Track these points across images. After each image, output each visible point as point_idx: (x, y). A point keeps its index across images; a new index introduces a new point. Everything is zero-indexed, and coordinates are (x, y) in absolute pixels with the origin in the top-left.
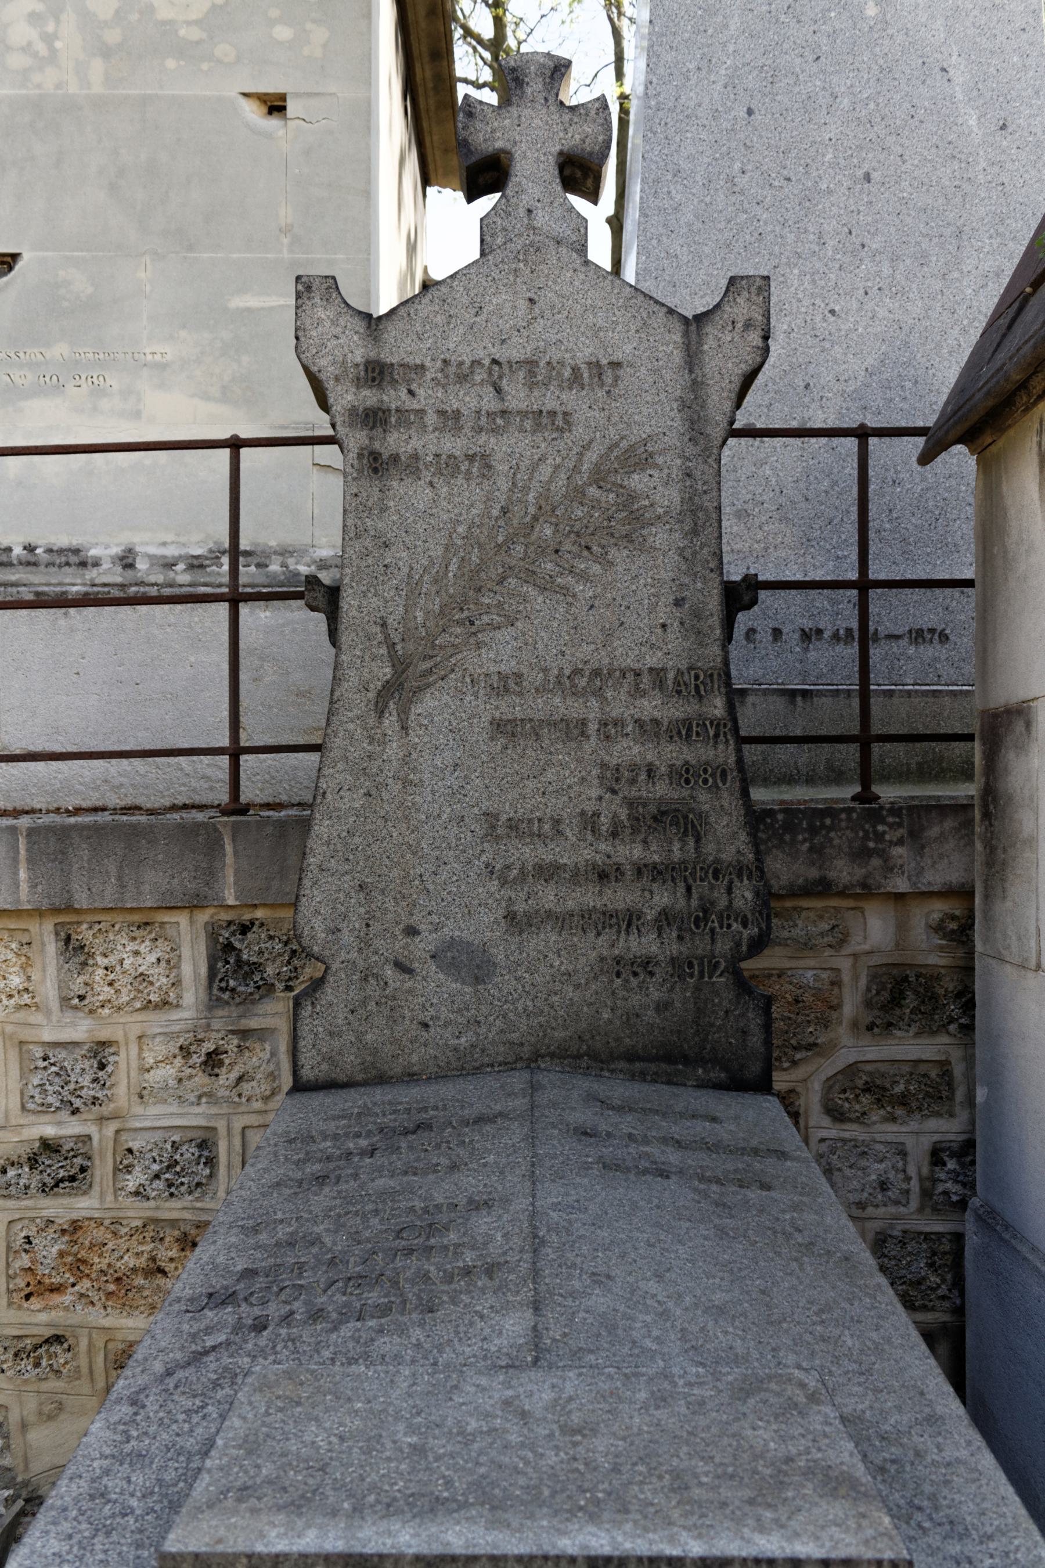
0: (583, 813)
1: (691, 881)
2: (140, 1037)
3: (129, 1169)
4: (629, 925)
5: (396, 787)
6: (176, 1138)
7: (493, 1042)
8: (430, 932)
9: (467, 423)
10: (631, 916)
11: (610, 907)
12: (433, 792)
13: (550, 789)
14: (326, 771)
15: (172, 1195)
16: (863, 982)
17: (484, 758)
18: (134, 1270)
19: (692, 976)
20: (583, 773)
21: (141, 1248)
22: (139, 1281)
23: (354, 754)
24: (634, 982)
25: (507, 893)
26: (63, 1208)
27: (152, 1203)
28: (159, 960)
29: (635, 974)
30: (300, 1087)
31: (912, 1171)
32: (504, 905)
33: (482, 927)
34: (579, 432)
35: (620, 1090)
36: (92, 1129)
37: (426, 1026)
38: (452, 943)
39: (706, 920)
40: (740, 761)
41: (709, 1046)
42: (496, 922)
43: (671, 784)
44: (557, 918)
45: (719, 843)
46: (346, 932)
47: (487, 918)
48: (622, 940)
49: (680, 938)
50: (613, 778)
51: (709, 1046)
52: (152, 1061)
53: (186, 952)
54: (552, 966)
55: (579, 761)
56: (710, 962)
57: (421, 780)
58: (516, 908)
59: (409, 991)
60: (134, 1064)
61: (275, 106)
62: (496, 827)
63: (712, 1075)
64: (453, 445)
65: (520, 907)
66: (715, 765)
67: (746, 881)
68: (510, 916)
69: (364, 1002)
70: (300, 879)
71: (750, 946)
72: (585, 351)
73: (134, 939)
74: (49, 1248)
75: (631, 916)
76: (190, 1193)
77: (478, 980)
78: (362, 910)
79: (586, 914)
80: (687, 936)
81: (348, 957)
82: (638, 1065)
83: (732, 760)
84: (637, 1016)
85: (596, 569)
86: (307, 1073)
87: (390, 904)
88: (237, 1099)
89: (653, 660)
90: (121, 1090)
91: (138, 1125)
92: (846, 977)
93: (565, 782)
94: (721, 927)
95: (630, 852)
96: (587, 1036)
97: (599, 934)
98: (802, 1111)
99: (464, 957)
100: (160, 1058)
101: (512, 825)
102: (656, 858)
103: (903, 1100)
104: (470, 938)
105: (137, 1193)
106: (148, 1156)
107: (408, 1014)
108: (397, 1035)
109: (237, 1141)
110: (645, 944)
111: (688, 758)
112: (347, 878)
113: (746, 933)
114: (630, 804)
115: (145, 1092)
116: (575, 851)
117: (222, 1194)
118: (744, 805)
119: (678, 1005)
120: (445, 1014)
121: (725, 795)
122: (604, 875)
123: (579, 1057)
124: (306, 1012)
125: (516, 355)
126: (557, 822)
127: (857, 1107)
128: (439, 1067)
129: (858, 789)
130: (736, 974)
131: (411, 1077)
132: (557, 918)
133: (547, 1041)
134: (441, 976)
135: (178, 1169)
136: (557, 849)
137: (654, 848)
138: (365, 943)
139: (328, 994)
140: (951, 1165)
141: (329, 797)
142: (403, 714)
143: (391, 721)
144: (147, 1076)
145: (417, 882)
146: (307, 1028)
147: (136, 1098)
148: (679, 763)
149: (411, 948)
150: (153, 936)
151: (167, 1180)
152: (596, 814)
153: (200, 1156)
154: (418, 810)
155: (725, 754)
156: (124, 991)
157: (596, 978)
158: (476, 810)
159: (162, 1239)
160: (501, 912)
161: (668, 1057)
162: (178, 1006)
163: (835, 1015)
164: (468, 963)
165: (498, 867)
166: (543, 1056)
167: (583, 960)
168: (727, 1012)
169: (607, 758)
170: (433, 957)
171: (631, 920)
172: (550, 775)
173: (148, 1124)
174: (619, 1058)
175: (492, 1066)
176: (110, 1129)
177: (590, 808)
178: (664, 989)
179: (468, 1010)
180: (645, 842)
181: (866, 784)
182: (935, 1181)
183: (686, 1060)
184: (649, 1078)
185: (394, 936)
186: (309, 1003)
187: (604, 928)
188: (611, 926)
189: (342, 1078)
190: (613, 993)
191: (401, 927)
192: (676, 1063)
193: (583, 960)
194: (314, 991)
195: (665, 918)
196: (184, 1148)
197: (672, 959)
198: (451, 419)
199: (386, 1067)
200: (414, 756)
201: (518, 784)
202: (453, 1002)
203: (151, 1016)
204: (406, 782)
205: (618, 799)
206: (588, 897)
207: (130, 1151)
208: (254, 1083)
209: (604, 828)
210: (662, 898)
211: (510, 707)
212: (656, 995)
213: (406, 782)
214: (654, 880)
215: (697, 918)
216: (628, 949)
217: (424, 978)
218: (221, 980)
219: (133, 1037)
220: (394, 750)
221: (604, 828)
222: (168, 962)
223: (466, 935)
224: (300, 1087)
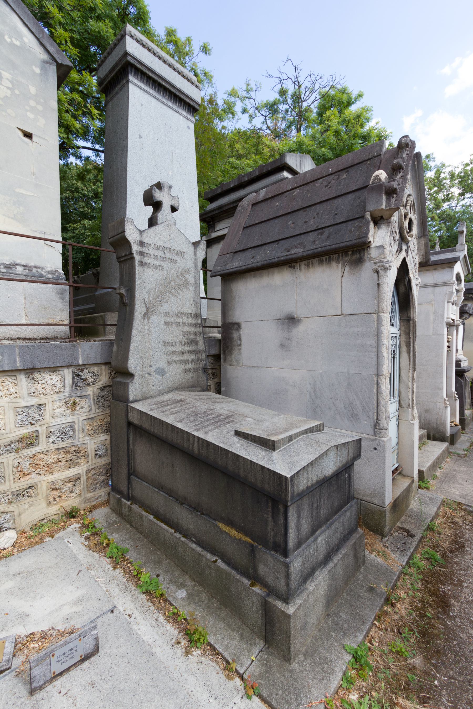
5: (147, 335)
6: (64, 426)
9: (159, 258)
18: (53, 463)
23: (139, 328)
25: (167, 357)
26: (30, 452)
33: (163, 364)
34: (178, 264)
36: (38, 428)
38: (158, 368)
47: (164, 362)
50: (185, 334)
61: (28, 135)
62: (167, 344)
64: (156, 263)
65: (170, 360)
68: (168, 362)
72: (179, 249)
74: (26, 464)
79: (180, 361)
85: (181, 292)
89: (190, 312)
93: (176, 335)
95: (187, 348)
101: (168, 343)
110: (190, 366)
114: (187, 339)
116: (179, 348)
117: (77, 438)
120: (157, 383)
122: (183, 353)
125: (167, 246)
131: (151, 397)
138: (142, 369)
142: (148, 319)
143: (146, 321)
155: (200, 330)
164: (161, 372)
171: (186, 362)
172: (174, 333)
176: (45, 427)
177: (181, 340)
183: (196, 387)
198: (156, 257)
203: (58, 395)
204: (149, 334)
206: (181, 357)
210: (192, 357)
211: (168, 319)
219: (50, 401)
220: (147, 327)
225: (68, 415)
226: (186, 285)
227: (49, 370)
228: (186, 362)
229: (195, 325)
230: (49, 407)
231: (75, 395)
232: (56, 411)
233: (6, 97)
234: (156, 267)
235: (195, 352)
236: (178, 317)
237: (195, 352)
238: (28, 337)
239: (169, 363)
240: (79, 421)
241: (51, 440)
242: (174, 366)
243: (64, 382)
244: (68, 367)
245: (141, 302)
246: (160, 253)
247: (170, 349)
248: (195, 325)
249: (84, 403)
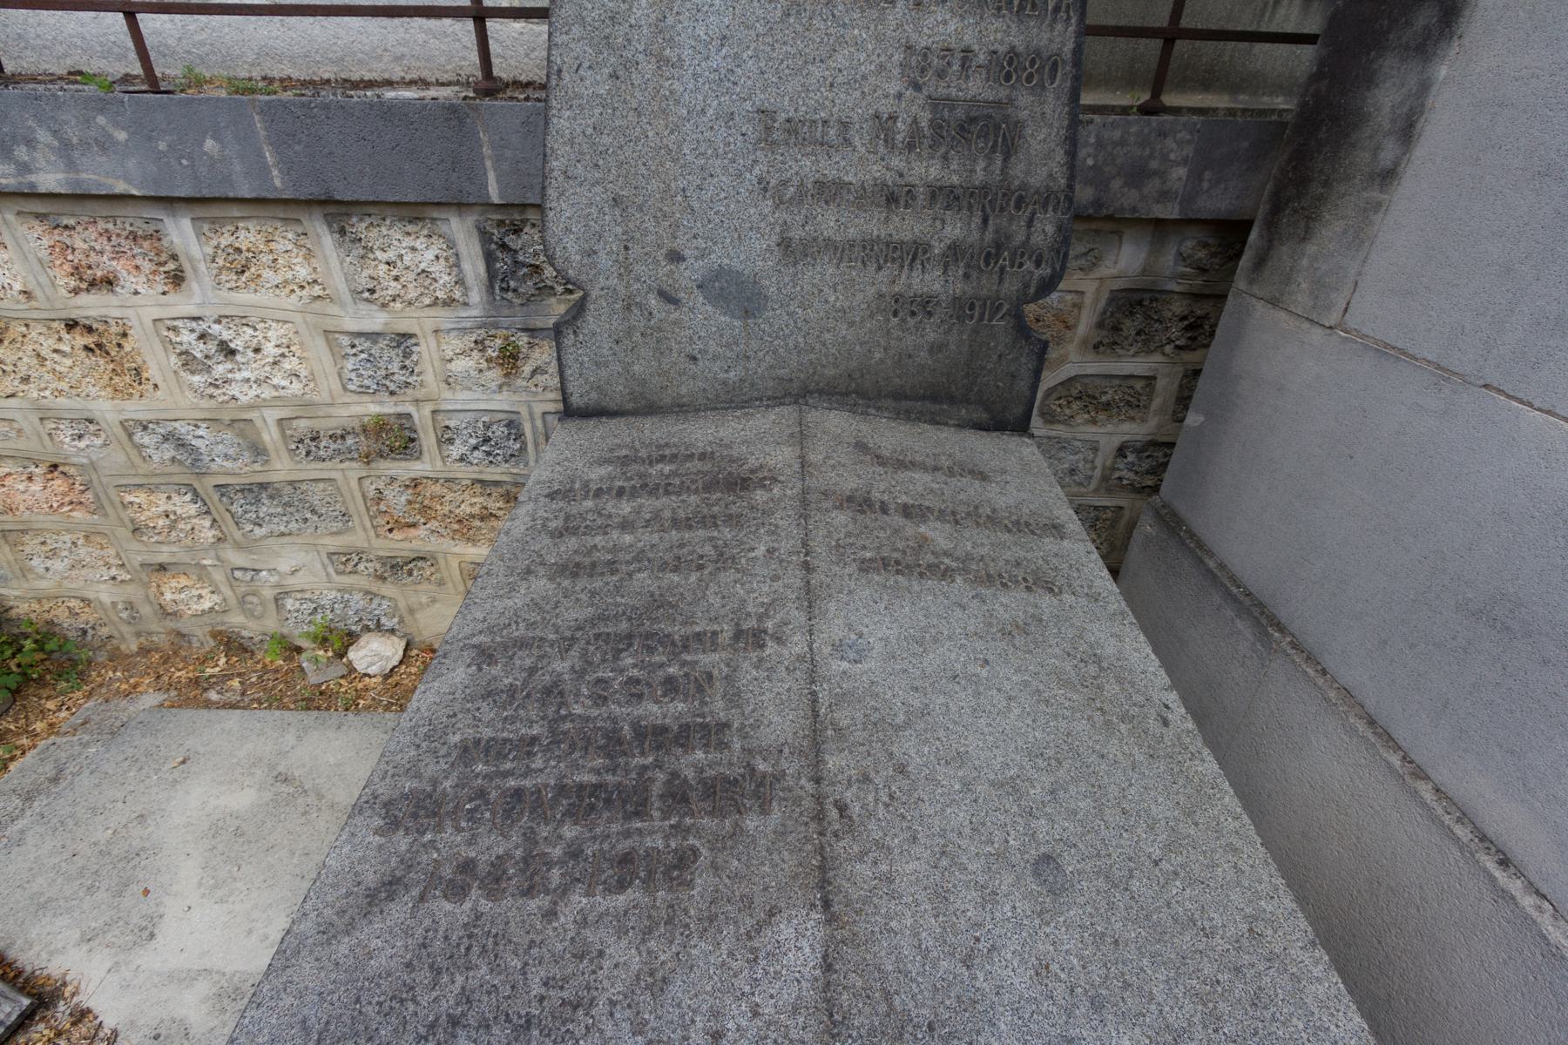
0: (877, 116)
1: (988, 210)
3: (451, 441)
4: (914, 259)
5: (648, 67)
7: (762, 378)
8: (696, 258)
12: (695, 76)
13: (840, 79)
14: (560, 39)
16: (1103, 303)
17: (761, 30)
18: (473, 516)
20: (882, 59)
22: (477, 523)
24: (911, 322)
25: (783, 215)
28: (437, 257)
29: (913, 314)
30: (569, 412)
31: (1099, 462)
32: (778, 229)
33: (751, 254)
35: (890, 435)
36: (410, 409)
37: (694, 359)
38: (720, 273)
39: (998, 256)
40: (1078, 50)
42: (769, 249)
43: (988, 79)
44: (836, 248)
45: (1030, 164)
48: (904, 276)
49: (966, 276)
50: (921, 65)
53: (462, 248)
55: (879, 39)
56: (992, 304)
57: (680, 59)
58: (791, 234)
59: (675, 323)
60: (435, 356)
62: (777, 130)
65: (796, 234)
66: (1045, 55)
67: (1050, 214)
68: (785, 244)
69: (629, 332)
70: (544, 188)
71: (1037, 292)
73: (409, 234)
74: (398, 500)
77: (747, 314)
78: (619, 230)
79: (868, 244)
80: (974, 275)
82: (905, 404)
83: (1070, 46)
87: (649, 224)
90: (429, 377)
92: (1088, 300)
94: (1012, 266)
95: (927, 170)
97: (880, 268)
99: (733, 289)
101: (792, 128)
102: (955, 179)
103: (1107, 406)
105: (462, 459)
109: (539, 423)
110: (929, 281)
111: (1016, 42)
112: (598, 189)
113: (1038, 273)
114: (935, 103)
116: (862, 166)
118: (1069, 113)
119: (952, 347)
120: (713, 347)
121: (1050, 97)
123: (847, 394)
124: (569, 339)
126: (845, 125)
127: (1067, 412)
129: (1145, 97)
130: (1018, 316)
131: (681, 409)
134: (709, 308)
136: (843, 163)
137: (954, 166)
138: (626, 268)
139: (590, 322)
140: (1131, 458)
141: (566, 75)
144: (449, 366)
145: (679, 198)
148: (1002, 49)
149: (676, 276)
150: (425, 232)
152: (893, 118)
154: (677, 102)
157: (871, 316)
158: (748, 105)
160: (775, 238)
161: (934, 398)
162: (466, 304)
163: (1069, 334)
164: (737, 294)
165: (773, 182)
166: (811, 393)
167: (860, 296)
169: (914, 36)
170: (699, 287)
171: (915, 253)
172: (841, 59)
173: (459, 407)
174: (886, 396)
176: (427, 410)
177: (885, 107)
180: (945, 158)
181: (1156, 94)
182: (1114, 469)
183: (952, 400)
188: (894, 259)
189: (613, 406)
190: (888, 332)
191: (664, 251)
193: (860, 296)
194: (575, 318)
195: (955, 251)
197: (955, 299)
200: (670, 20)
201: (800, 70)
204: (662, 61)
205: (921, 98)
206: (872, 224)
209: (899, 137)
210: (954, 229)
212: (931, 336)
213: (662, 61)
214: (948, 207)
215: (989, 255)
216: (910, 286)
217: (691, 310)
221: (899, 137)
222: (447, 259)
224: (569, 412)
225: (494, 386)
230: (426, 350)
232: (453, 366)
238: (523, 78)
240: (531, 414)
241: (456, 450)
243: (457, 265)
244: (461, 206)
249: (545, 357)
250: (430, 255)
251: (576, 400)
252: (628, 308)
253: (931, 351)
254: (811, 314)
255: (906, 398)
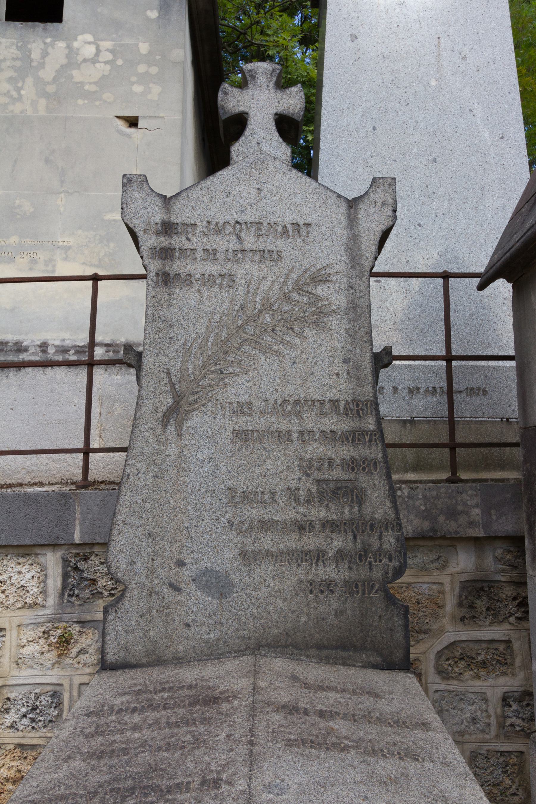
0: (289, 488)
1: (355, 531)
2: (19, 626)
4: (318, 560)
5: (173, 472)
6: (37, 691)
8: (192, 564)
9: (221, 256)
10: (319, 554)
11: (306, 548)
12: (196, 475)
13: (269, 473)
14: (130, 462)
15: (33, 728)
16: (457, 590)
17: (228, 454)
19: (358, 592)
20: (289, 464)
21: (12, 764)
22: (10, 786)
23: (148, 451)
24: (321, 597)
27: (20, 734)
28: (33, 577)
29: (322, 592)
31: (491, 711)
32: (239, 546)
33: (224, 559)
34: (287, 262)
35: (313, 671)
37: (188, 626)
38: (206, 572)
39: (366, 556)
40: (385, 456)
41: (369, 640)
42: (234, 557)
43: (343, 470)
44: (273, 555)
45: (373, 508)
46: (138, 564)
47: (229, 555)
48: (313, 569)
49: (350, 568)
50: (308, 467)
51: (369, 640)
52: (25, 641)
54: (269, 586)
55: (287, 456)
56: (369, 584)
57: (189, 468)
58: (247, 549)
59: (178, 603)
61: (133, 122)
62: (236, 497)
63: (372, 659)
64: (212, 269)
65: (250, 548)
66: (369, 459)
67: (390, 532)
68: (243, 554)
69: (149, 610)
70: (111, 530)
71: (394, 574)
72: (290, 218)
73: (19, 564)
75: (319, 554)
76: (45, 727)
77: (222, 595)
78: (150, 550)
80: (354, 567)
81: (140, 580)
82: (325, 652)
83: (380, 455)
84: (324, 619)
85: (296, 341)
86: (110, 658)
87: (167, 546)
88: (76, 665)
89: (331, 395)
91: (14, 682)
92: (447, 588)
93: (278, 469)
94: (376, 561)
95: (317, 513)
96: (291, 633)
97: (299, 565)
98: (423, 672)
99: (213, 581)
100: (31, 639)
101: (245, 495)
102: (334, 517)
103: (484, 664)
104: (218, 568)
105: (12, 727)
106: (20, 702)
107: (177, 618)
108: (170, 632)
110: (328, 572)
111: (353, 454)
112: (141, 529)
113: (391, 565)
114: (318, 482)
115: (20, 661)
116: (284, 512)
118: (388, 483)
119: (349, 612)
120: (200, 618)
121: (377, 477)
122: (302, 527)
123: (286, 647)
124: (112, 616)
125: (249, 219)
126: (273, 494)
127: (457, 670)
128: (196, 653)
130: (386, 591)
131: (178, 661)
132: (273, 555)
133: (266, 636)
134: (199, 593)
135: (38, 711)
136: (273, 511)
137: (333, 510)
138: (151, 571)
139: (127, 605)
140: (515, 706)
141: (131, 477)
142: (179, 425)
143: (171, 431)
144: (22, 651)
145: (185, 532)
146: (111, 628)
147: (14, 665)
148: (348, 458)
149: (180, 574)
150: (30, 562)
151: (31, 718)
152: (297, 489)
153: (52, 702)
154: (186, 486)
155: (375, 452)
156: (11, 596)
157: (297, 594)
158: (222, 486)
159: (25, 758)
160: (238, 551)
161: (343, 647)
162: (44, 606)
163: (441, 612)
164: (216, 585)
165: (236, 522)
166: (263, 646)
167: (289, 583)
168: (380, 617)
169: (303, 454)
170: (194, 580)
171: (318, 556)
173: (21, 682)
174: (311, 647)
175: (231, 653)
177: (293, 485)
178: (340, 601)
179: (215, 615)
180: (327, 506)
181: (454, 473)
182: (506, 717)
183: (355, 648)
184: (331, 661)
185: (169, 567)
186: (113, 611)
187: (302, 562)
188: (306, 561)
189: (133, 661)
190: (308, 604)
191: (174, 560)
192: (348, 650)
193: (289, 583)
195: (341, 555)
196: (42, 697)
197: (345, 582)
198: (211, 254)
199: (162, 654)
200: (185, 452)
201: (249, 470)
202: (206, 610)
203: (26, 612)
204: (180, 469)
205: (310, 480)
206: (293, 541)
207: (8, 699)
208: (87, 655)
209: (302, 498)
210: (339, 542)
211: (243, 423)
212: (335, 606)
213: (180, 469)
214: (333, 531)
215: (360, 556)
216: (317, 575)
217: (188, 595)
218: (71, 590)
219: (14, 625)
220: (172, 449)
221: (302, 498)
222: (39, 578)
223: (215, 567)
225: (49, 664)
226: (318, 315)
227: (16, 550)
228: (318, 556)
229: (354, 437)
231: (66, 617)
232: (23, 651)
233: (103, 77)
234: (209, 281)
235: (354, 527)
236: (285, 414)
237: (354, 527)
238: (100, 479)
239: (246, 557)
240: (71, 685)
242: (267, 568)
243: (44, 582)
244: (54, 546)
245: (159, 380)
246: (223, 243)
247: (253, 513)
248: (354, 437)
249: (89, 642)
250: (29, 576)
251: (110, 658)
252: (150, 595)
253: (336, 615)
254: (260, 594)
255: (325, 647)
